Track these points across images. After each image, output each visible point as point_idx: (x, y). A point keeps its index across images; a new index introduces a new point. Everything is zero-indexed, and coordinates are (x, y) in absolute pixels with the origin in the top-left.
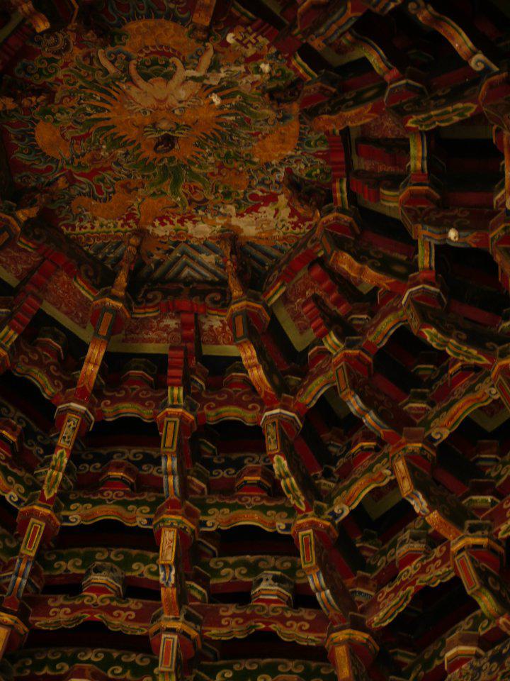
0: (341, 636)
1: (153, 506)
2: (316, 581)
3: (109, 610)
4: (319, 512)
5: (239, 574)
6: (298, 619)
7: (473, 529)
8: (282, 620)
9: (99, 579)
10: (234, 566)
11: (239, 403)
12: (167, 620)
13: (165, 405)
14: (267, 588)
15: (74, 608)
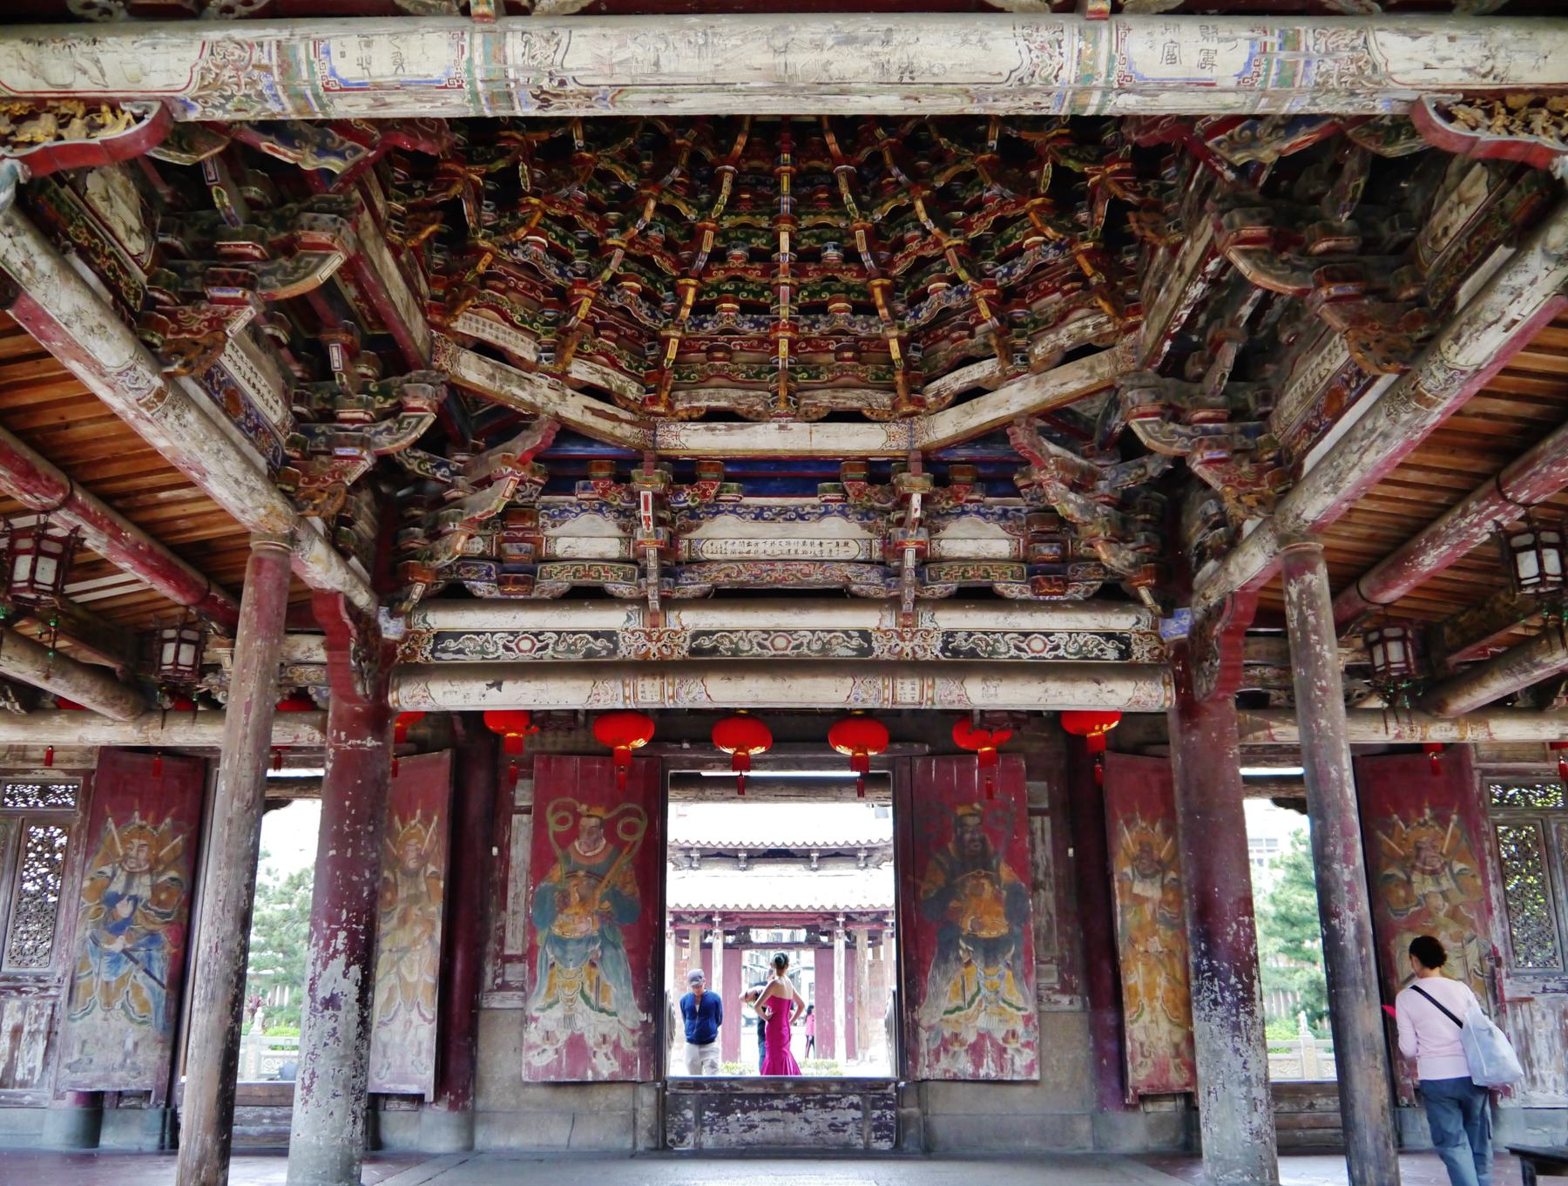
0: (877, 282)
1: (770, 215)
2: (862, 248)
3: (745, 270)
4: (866, 219)
5: (812, 242)
6: (849, 270)
7: (956, 235)
8: (842, 271)
9: (737, 252)
10: (808, 237)
11: (822, 160)
12: (782, 278)
13: (779, 164)
14: (832, 254)
15: (726, 270)
